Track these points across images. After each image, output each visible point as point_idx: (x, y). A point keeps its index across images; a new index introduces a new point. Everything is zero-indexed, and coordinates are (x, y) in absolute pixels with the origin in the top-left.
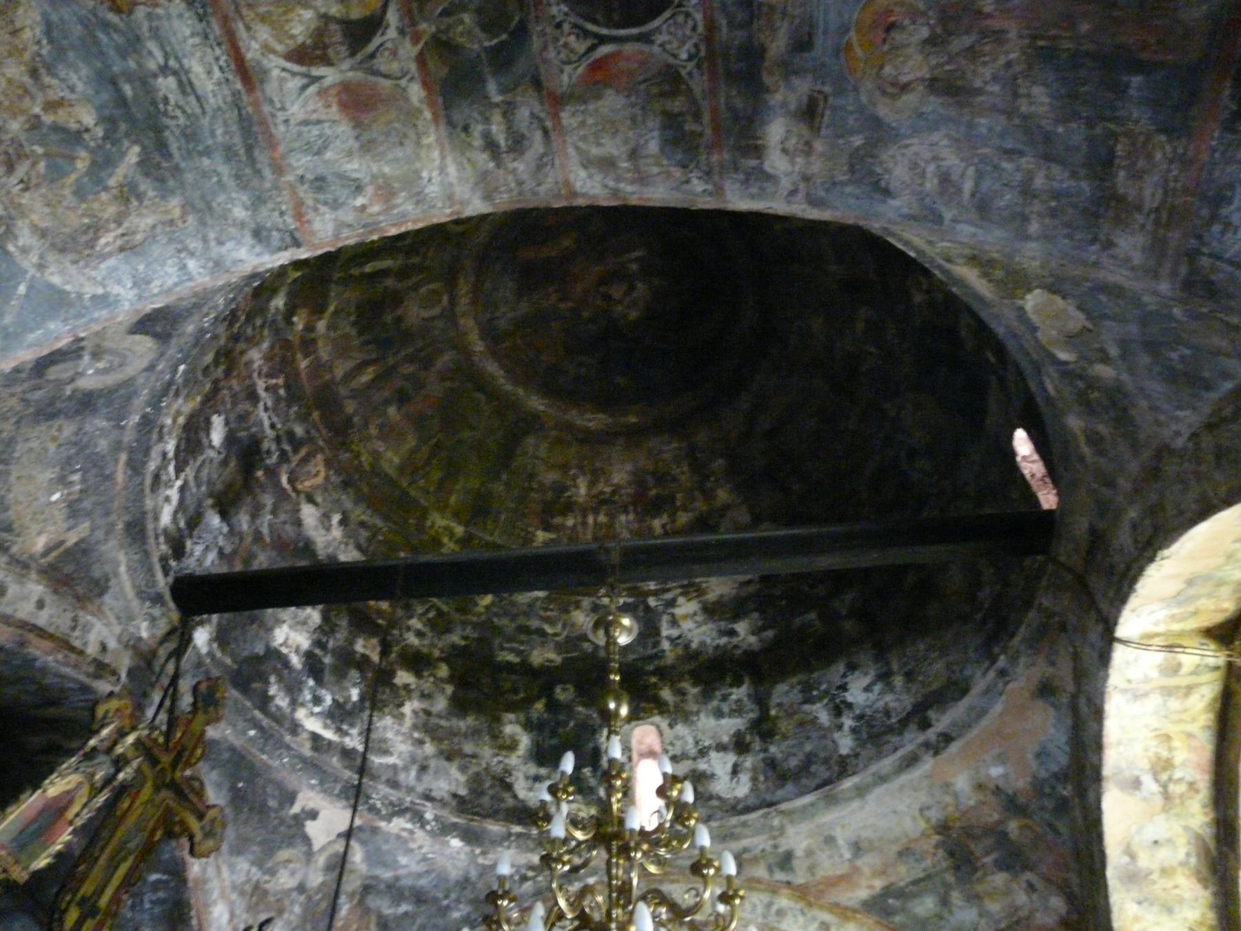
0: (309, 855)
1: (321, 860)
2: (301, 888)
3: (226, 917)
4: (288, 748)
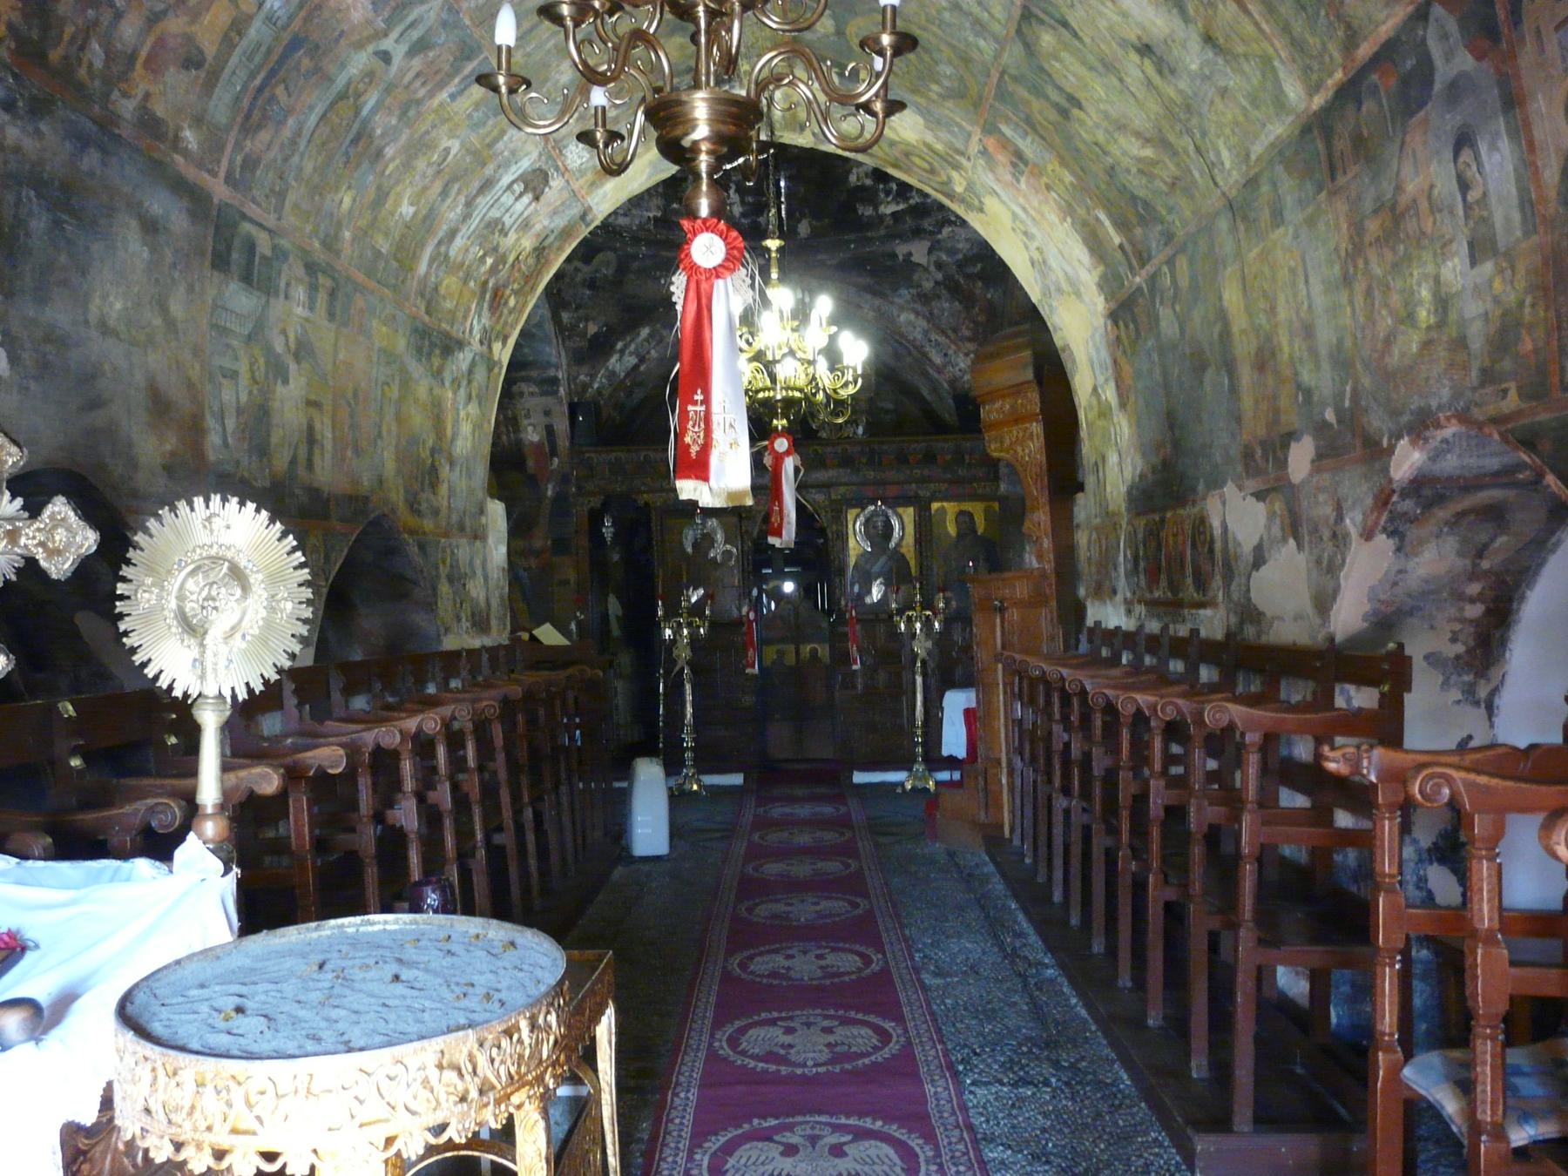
0: (926, 269)
1: (932, 268)
2: (937, 283)
3: (912, 317)
4: (871, 239)
